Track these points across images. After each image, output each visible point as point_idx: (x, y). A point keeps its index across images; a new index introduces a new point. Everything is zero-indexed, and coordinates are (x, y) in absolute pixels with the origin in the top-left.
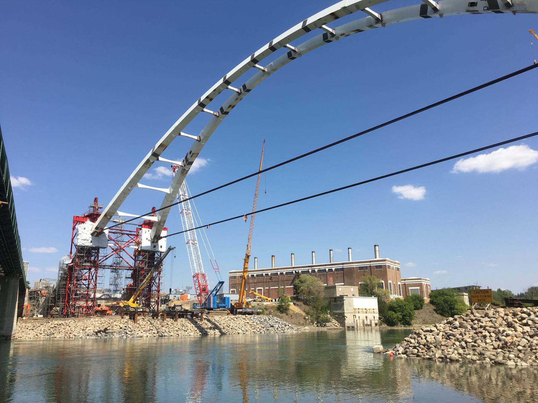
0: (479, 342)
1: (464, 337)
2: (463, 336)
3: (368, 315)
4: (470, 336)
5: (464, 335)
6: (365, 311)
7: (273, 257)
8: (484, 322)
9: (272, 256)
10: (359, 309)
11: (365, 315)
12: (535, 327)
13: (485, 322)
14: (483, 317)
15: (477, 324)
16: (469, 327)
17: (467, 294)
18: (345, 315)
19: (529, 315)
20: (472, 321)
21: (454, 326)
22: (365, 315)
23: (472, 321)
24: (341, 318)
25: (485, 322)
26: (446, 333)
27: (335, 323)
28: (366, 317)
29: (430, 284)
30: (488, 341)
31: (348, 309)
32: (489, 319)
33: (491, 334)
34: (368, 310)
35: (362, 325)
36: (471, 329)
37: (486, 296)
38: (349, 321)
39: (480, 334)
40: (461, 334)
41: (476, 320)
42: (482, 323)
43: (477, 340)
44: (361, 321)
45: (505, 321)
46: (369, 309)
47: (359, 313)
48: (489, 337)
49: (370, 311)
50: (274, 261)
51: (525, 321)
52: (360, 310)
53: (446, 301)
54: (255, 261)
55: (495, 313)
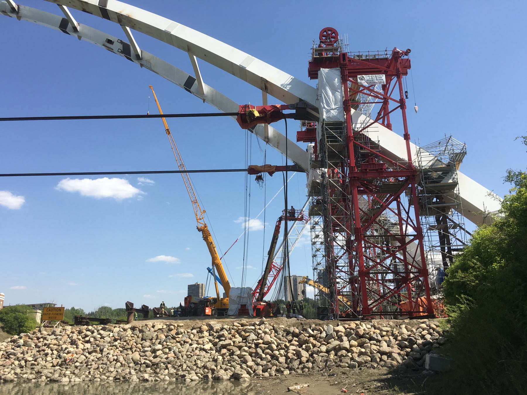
0: (40, 360)
1: (25, 356)
2: (24, 355)
4: (32, 354)
5: (25, 353)
8: (49, 340)
12: (95, 344)
13: (51, 340)
14: (50, 335)
15: (42, 342)
16: (33, 345)
17: (40, 312)
19: (93, 332)
20: (38, 338)
21: (18, 344)
23: (38, 338)
25: (51, 340)
26: (7, 353)
29: (3, 299)
30: (49, 358)
32: (55, 337)
33: (53, 352)
36: (34, 347)
37: (57, 314)
39: (42, 353)
40: (23, 353)
41: (42, 338)
42: (47, 340)
43: (38, 358)
45: (70, 338)
48: (51, 354)
51: (87, 339)
53: (16, 318)
55: (62, 330)
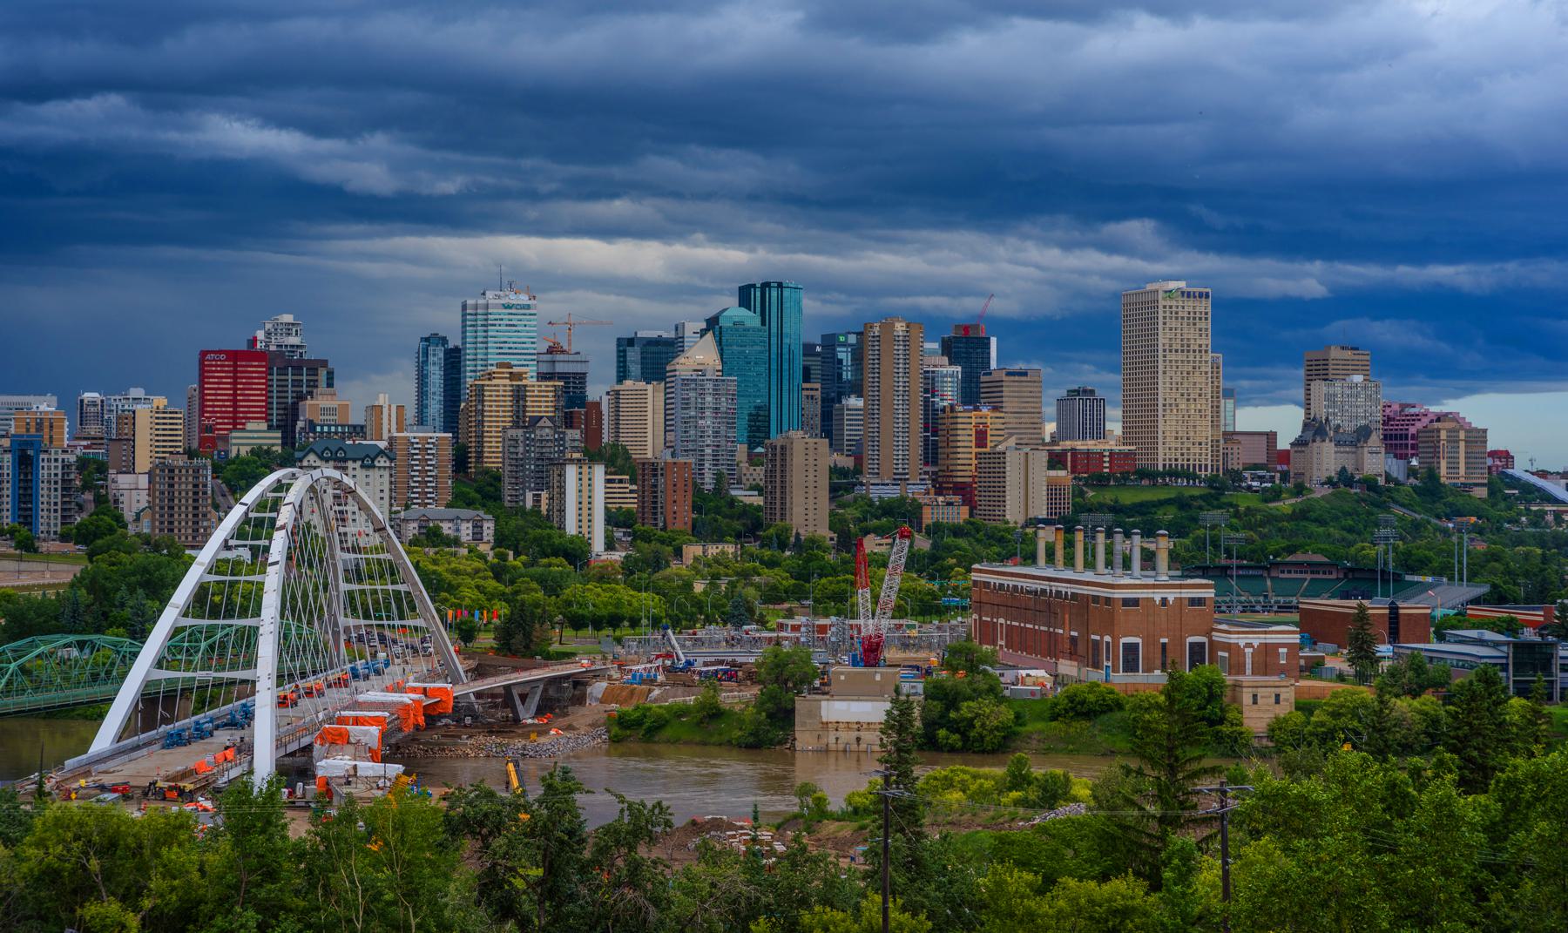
3: (863, 734)
6: (856, 726)
10: (838, 722)
28: (858, 739)
34: (865, 726)
49: (872, 726)
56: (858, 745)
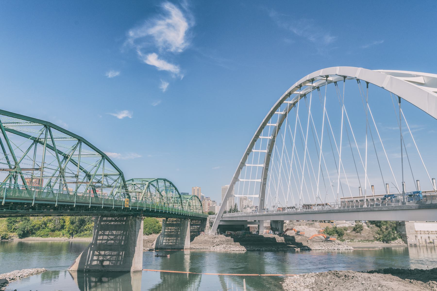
3: (430, 235)
6: (427, 232)
7: (373, 187)
9: (372, 186)
10: (420, 231)
11: (427, 235)
18: (407, 235)
22: (427, 235)
24: (404, 237)
27: (400, 241)
31: (410, 231)
34: (430, 232)
35: (424, 243)
38: (411, 240)
44: (423, 240)
46: (431, 231)
47: (421, 234)
49: (433, 232)
50: (374, 190)
52: (422, 232)
54: (359, 190)
56: (429, 239)
